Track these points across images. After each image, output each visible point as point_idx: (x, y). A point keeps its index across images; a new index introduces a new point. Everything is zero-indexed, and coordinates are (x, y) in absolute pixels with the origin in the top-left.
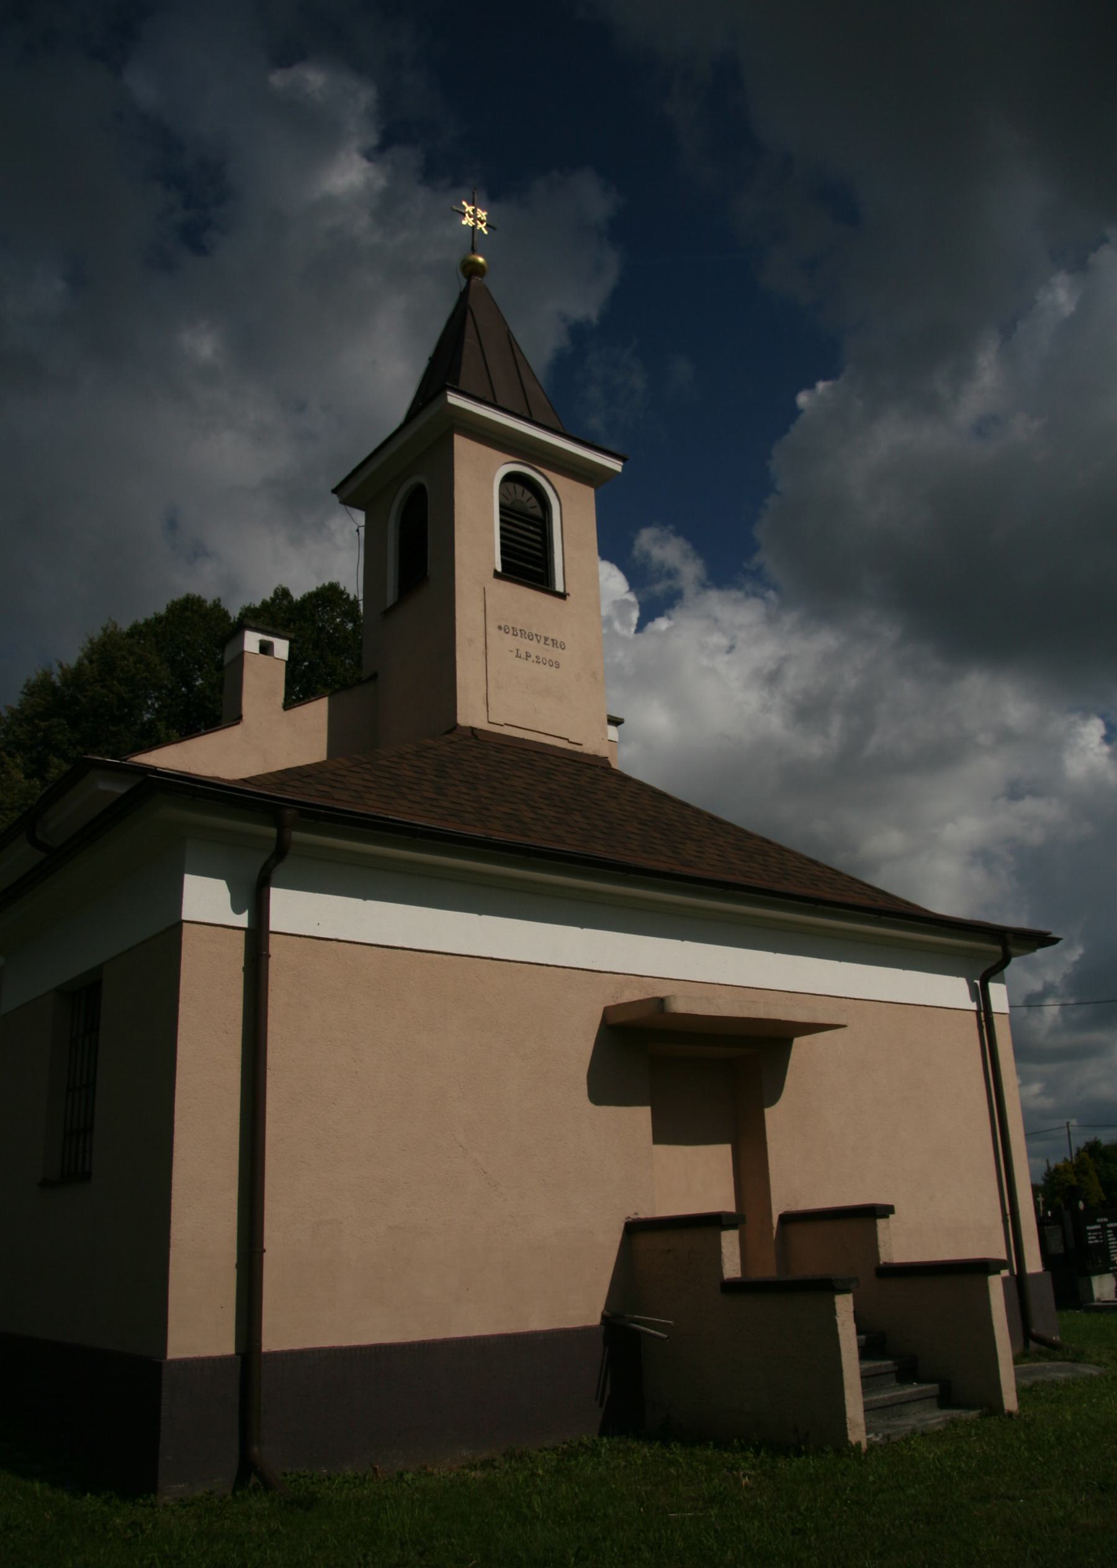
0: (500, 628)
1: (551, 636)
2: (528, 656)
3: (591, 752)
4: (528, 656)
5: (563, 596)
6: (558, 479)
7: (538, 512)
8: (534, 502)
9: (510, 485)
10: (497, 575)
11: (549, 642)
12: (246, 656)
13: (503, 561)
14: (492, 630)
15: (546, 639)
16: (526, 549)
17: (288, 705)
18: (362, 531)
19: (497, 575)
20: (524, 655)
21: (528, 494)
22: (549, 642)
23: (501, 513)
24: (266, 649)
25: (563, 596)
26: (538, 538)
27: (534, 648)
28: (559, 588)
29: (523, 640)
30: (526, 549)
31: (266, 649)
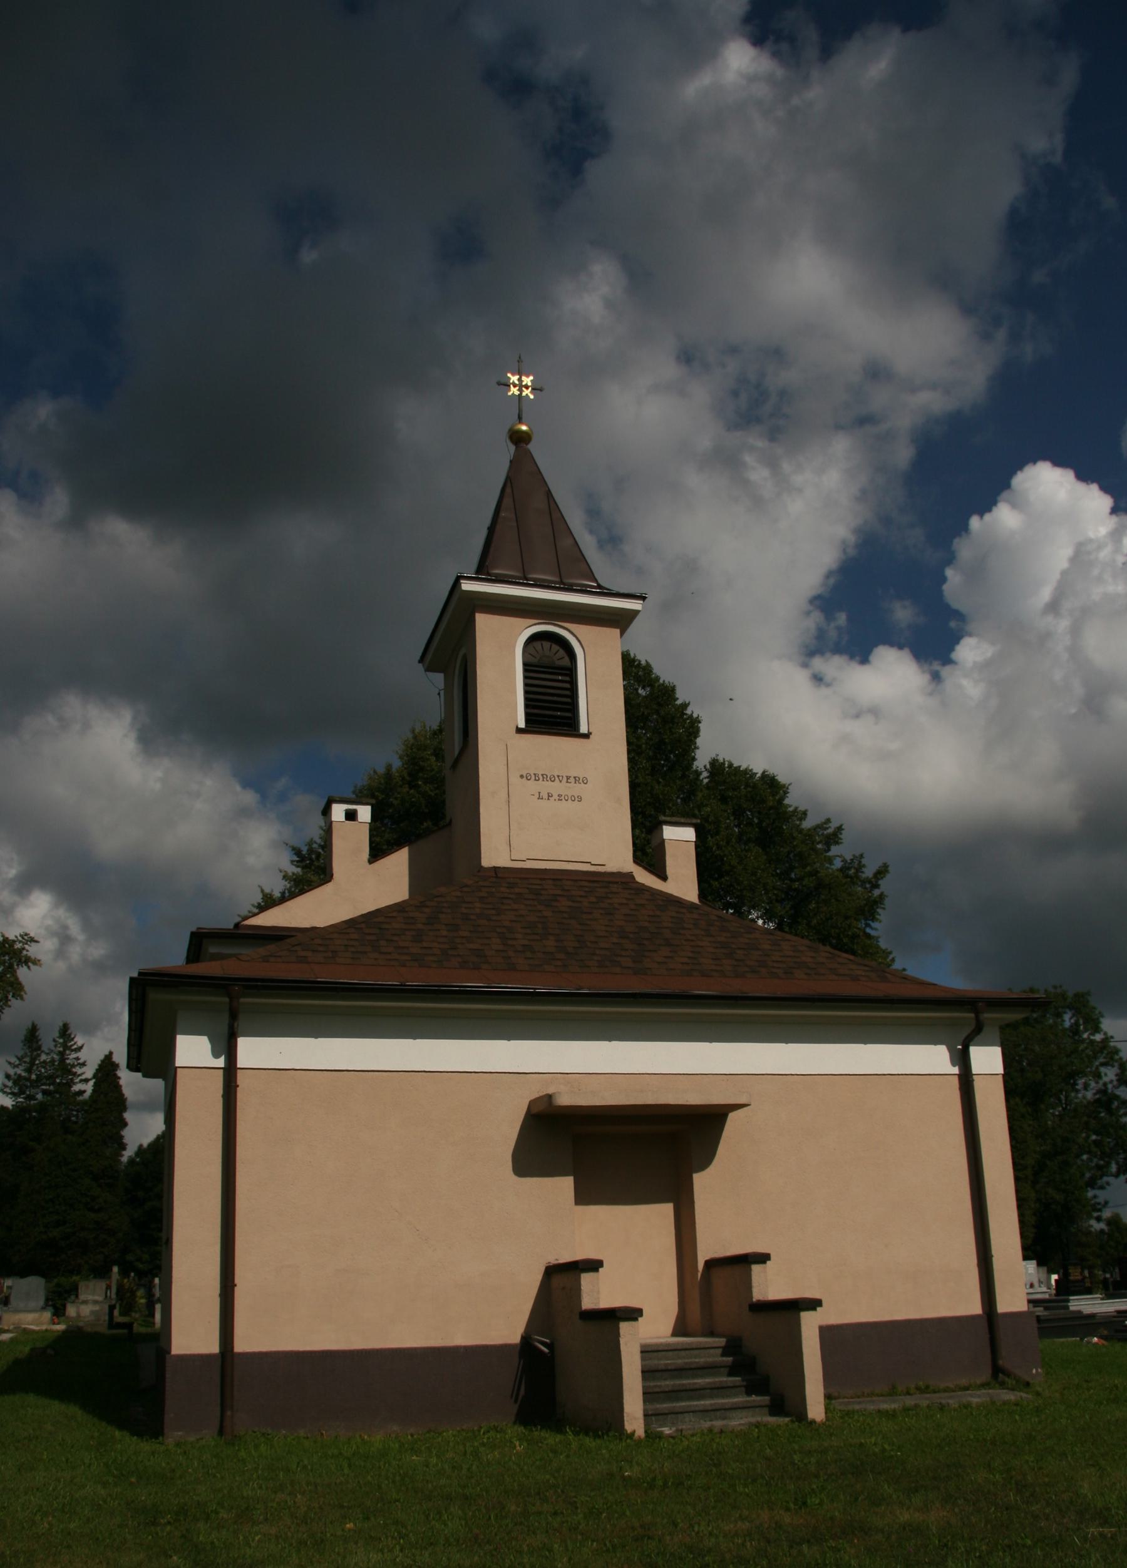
0: (522, 776)
1: (573, 774)
2: (550, 796)
3: (614, 870)
4: (550, 796)
5: (587, 736)
6: (582, 630)
7: (566, 662)
8: (562, 653)
9: (538, 645)
10: (519, 731)
11: (572, 780)
12: (334, 824)
13: (527, 715)
14: (515, 779)
15: (568, 778)
16: (555, 698)
17: (370, 862)
18: (442, 693)
19: (519, 731)
20: (546, 796)
21: (555, 647)
22: (572, 780)
23: (525, 670)
24: (351, 816)
25: (587, 736)
27: (556, 788)
28: (583, 729)
29: (545, 783)
30: (555, 698)
31: (351, 816)
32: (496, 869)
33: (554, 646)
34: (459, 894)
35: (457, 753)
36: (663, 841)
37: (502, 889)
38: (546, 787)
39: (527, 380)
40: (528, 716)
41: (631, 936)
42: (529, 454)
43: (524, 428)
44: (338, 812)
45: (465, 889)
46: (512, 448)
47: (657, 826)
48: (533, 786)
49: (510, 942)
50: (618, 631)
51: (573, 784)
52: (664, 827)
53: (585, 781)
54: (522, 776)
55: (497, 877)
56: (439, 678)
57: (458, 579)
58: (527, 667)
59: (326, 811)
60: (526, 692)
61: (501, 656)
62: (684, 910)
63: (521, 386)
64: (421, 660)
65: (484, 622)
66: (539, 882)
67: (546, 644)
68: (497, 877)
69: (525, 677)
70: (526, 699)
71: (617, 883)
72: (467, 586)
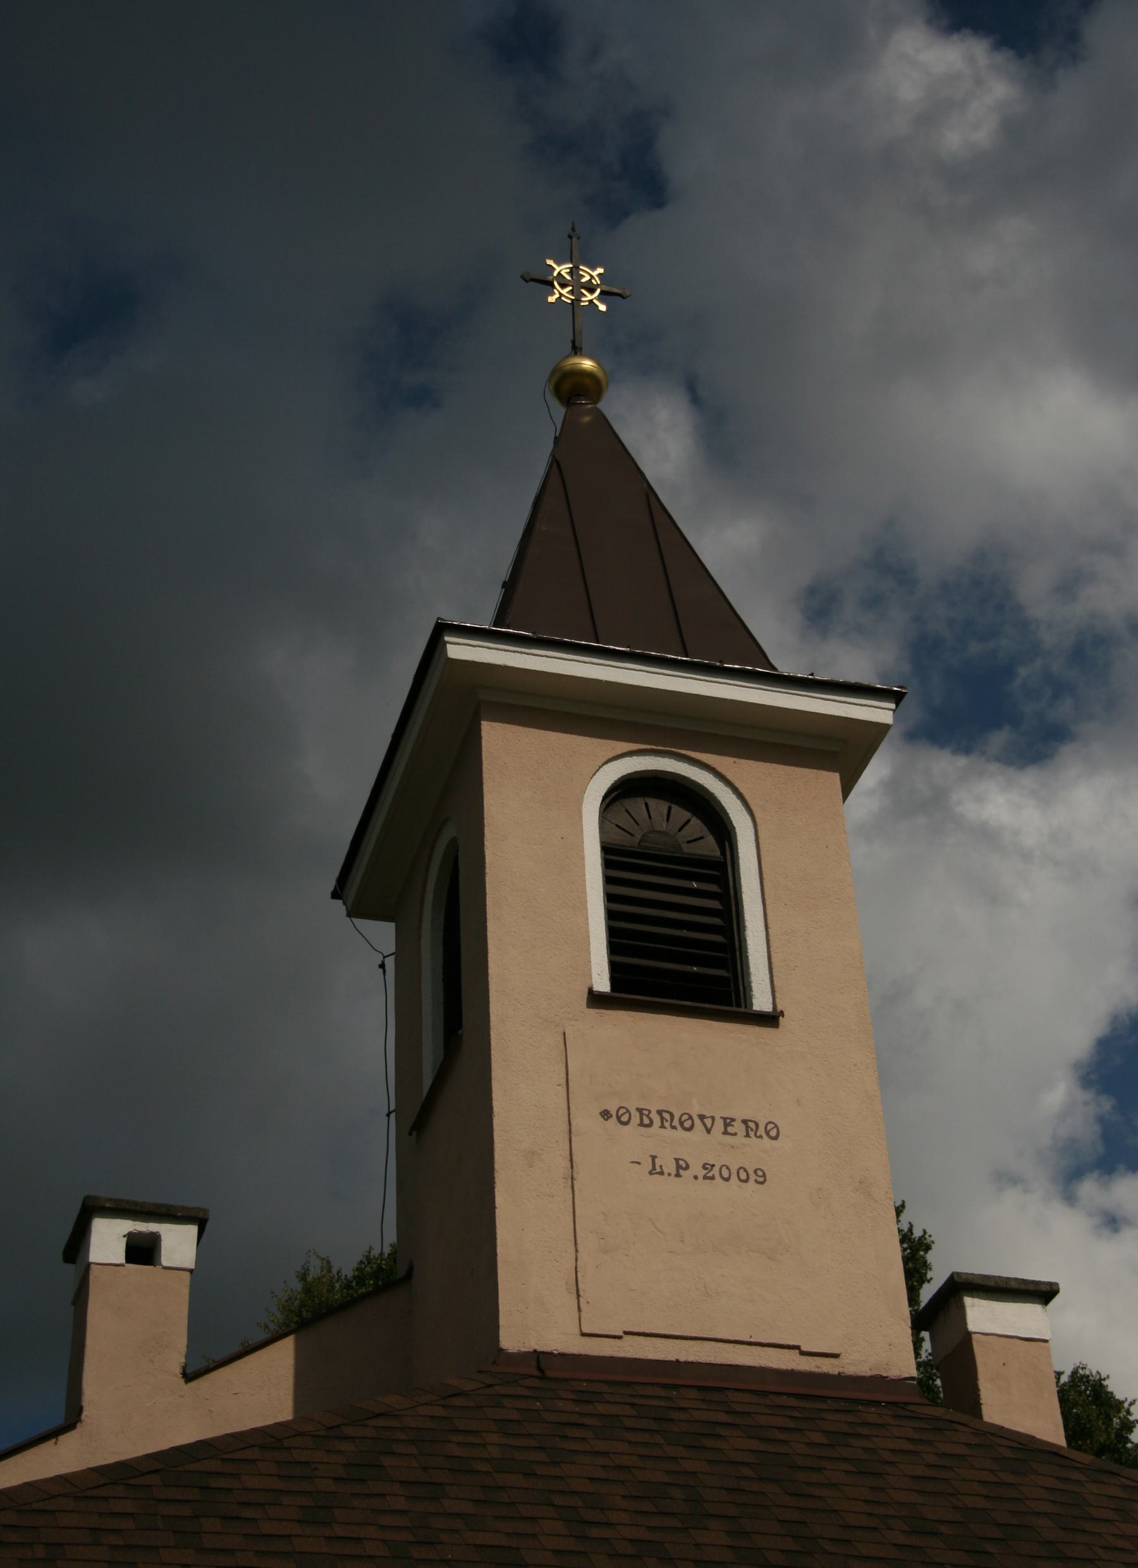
0: (606, 1114)
1: (739, 1114)
2: (681, 1167)
3: (865, 1370)
4: (681, 1167)
5: (771, 1019)
6: (750, 773)
7: (709, 847)
8: (696, 826)
9: (637, 806)
10: (596, 1000)
11: (738, 1127)
12: (94, 1272)
13: (614, 967)
14: (587, 1122)
15: (728, 1122)
16: (685, 933)
18: (390, 963)
19: (596, 1000)
20: (671, 1168)
21: (681, 814)
22: (738, 1127)
23: (607, 864)
24: (142, 1251)
25: (771, 1019)
26: (715, 904)
27: (696, 1146)
28: (761, 1002)
29: (668, 1132)
30: (685, 933)
31: (142, 1251)
32: (539, 1359)
33: (676, 809)
34: (439, 1412)
35: (427, 1082)
36: (968, 1336)
37: (561, 1404)
38: (669, 1143)
39: (592, 274)
40: (615, 969)
41: (944, 1529)
42: (603, 424)
43: (587, 364)
44: (108, 1239)
45: (456, 1401)
46: (559, 411)
47: (919, 1333)
48: (634, 1141)
49: (594, 1532)
50: (836, 777)
51: (740, 1139)
52: (968, 1301)
53: (773, 1132)
54: (606, 1114)
55: (543, 1377)
56: (383, 934)
57: (441, 629)
58: (611, 855)
59: (76, 1244)
60: (610, 915)
61: (547, 835)
62: (1075, 1475)
63: (578, 287)
64: (335, 895)
65: (498, 740)
66: (661, 1392)
67: (659, 807)
68: (543, 1377)
69: (608, 880)
70: (613, 933)
71: (876, 1403)
72: (459, 650)
